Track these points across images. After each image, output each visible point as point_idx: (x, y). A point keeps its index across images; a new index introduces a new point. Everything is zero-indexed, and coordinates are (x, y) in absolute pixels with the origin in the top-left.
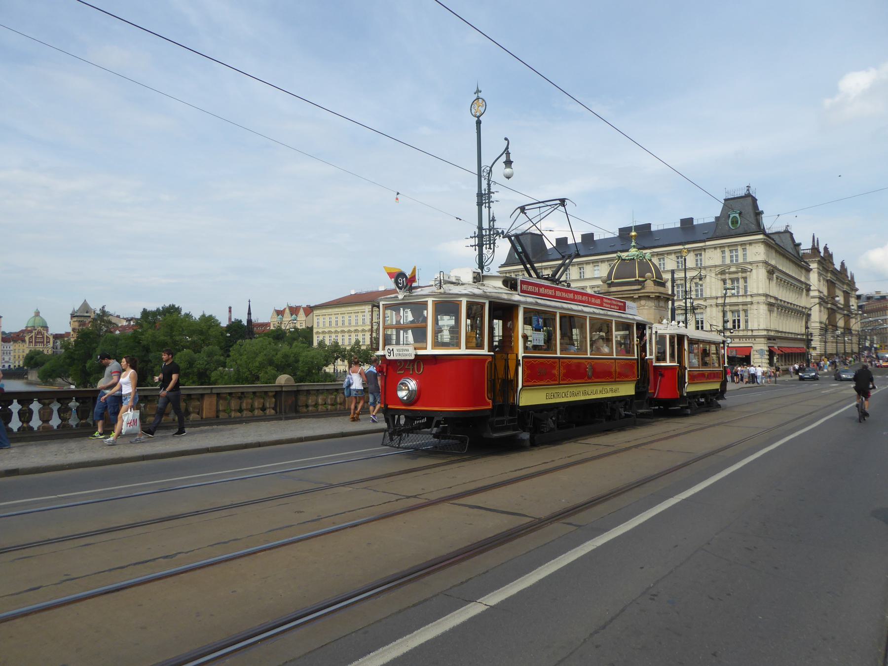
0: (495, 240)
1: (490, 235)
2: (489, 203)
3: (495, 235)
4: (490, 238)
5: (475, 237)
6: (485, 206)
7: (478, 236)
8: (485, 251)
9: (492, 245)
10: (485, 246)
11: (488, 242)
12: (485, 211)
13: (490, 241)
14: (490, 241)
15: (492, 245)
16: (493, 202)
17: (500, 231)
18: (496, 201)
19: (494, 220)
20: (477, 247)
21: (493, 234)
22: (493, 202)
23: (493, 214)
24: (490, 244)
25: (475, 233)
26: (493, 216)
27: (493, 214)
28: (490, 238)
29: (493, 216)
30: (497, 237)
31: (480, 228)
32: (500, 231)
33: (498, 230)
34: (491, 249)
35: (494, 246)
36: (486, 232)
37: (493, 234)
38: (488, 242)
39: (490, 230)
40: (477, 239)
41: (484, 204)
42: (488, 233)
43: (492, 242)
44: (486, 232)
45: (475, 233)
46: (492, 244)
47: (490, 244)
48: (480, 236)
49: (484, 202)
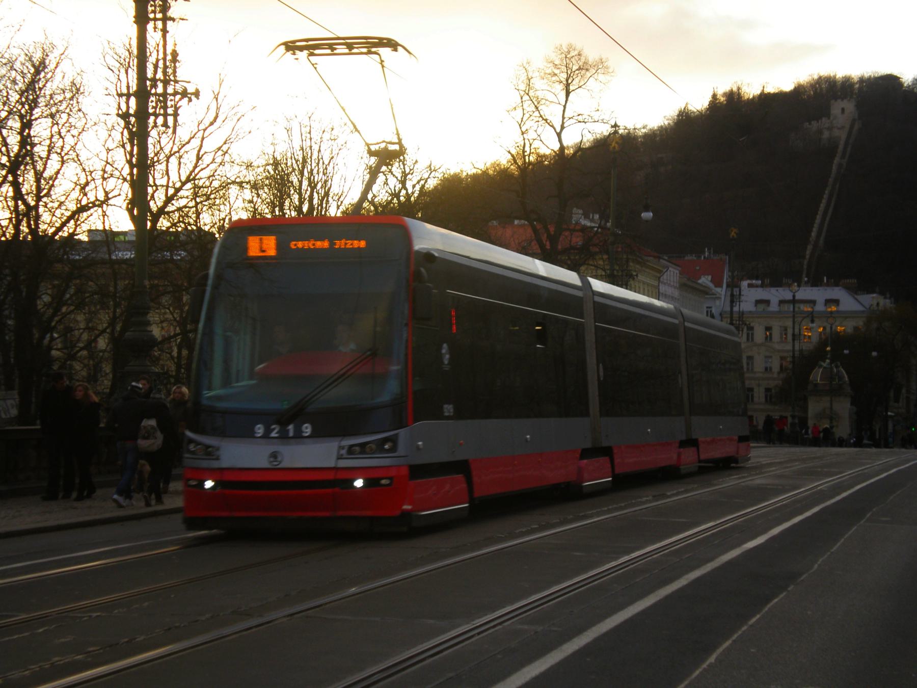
0: (176, 109)
2: (165, 19)
3: (178, 97)
6: (155, 28)
7: (136, 94)
9: (170, 120)
13: (165, 107)
15: (170, 120)
16: (174, 20)
19: (175, 59)
21: (175, 93)
22: (174, 20)
32: (191, 89)
35: (176, 121)
43: (170, 111)
47: (165, 115)
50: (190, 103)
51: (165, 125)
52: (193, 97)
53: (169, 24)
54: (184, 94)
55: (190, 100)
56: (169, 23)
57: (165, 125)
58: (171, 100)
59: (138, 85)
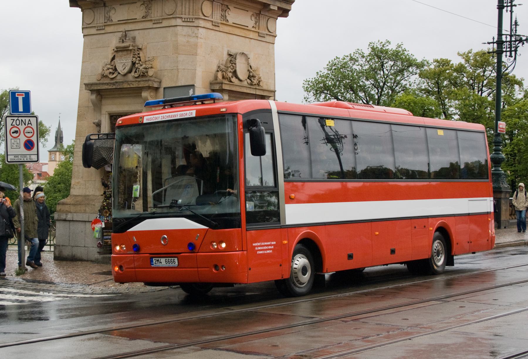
0: (516, 48)
1: (511, 41)
2: (512, 6)
3: (517, 42)
4: (511, 45)
5: (493, 43)
6: (507, 10)
8: (504, 59)
9: (513, 53)
10: (504, 54)
11: (508, 50)
12: (506, 15)
13: (510, 48)
14: (510, 48)
15: (513, 53)
17: (524, 38)
18: (519, 5)
20: (495, 55)
21: (515, 41)
23: (516, 18)
24: (511, 51)
25: (494, 39)
26: (516, 21)
27: (516, 18)
28: (511, 45)
29: (516, 21)
30: (520, 45)
31: (500, 34)
32: (524, 38)
33: (521, 36)
34: (512, 57)
36: (506, 38)
37: (515, 41)
38: (508, 50)
39: (511, 36)
40: (495, 45)
41: (506, 8)
42: (508, 39)
43: (513, 49)
44: (506, 38)
45: (494, 39)
46: (513, 51)
47: (511, 51)
48: (500, 43)
49: (505, 5)
50: (523, 45)
51: (510, 56)
52: (525, 42)
53: (514, 7)
54: (521, 41)
55: (523, 44)
56: (514, 7)
57: (510, 56)
58: (514, 44)
59: (498, 38)
